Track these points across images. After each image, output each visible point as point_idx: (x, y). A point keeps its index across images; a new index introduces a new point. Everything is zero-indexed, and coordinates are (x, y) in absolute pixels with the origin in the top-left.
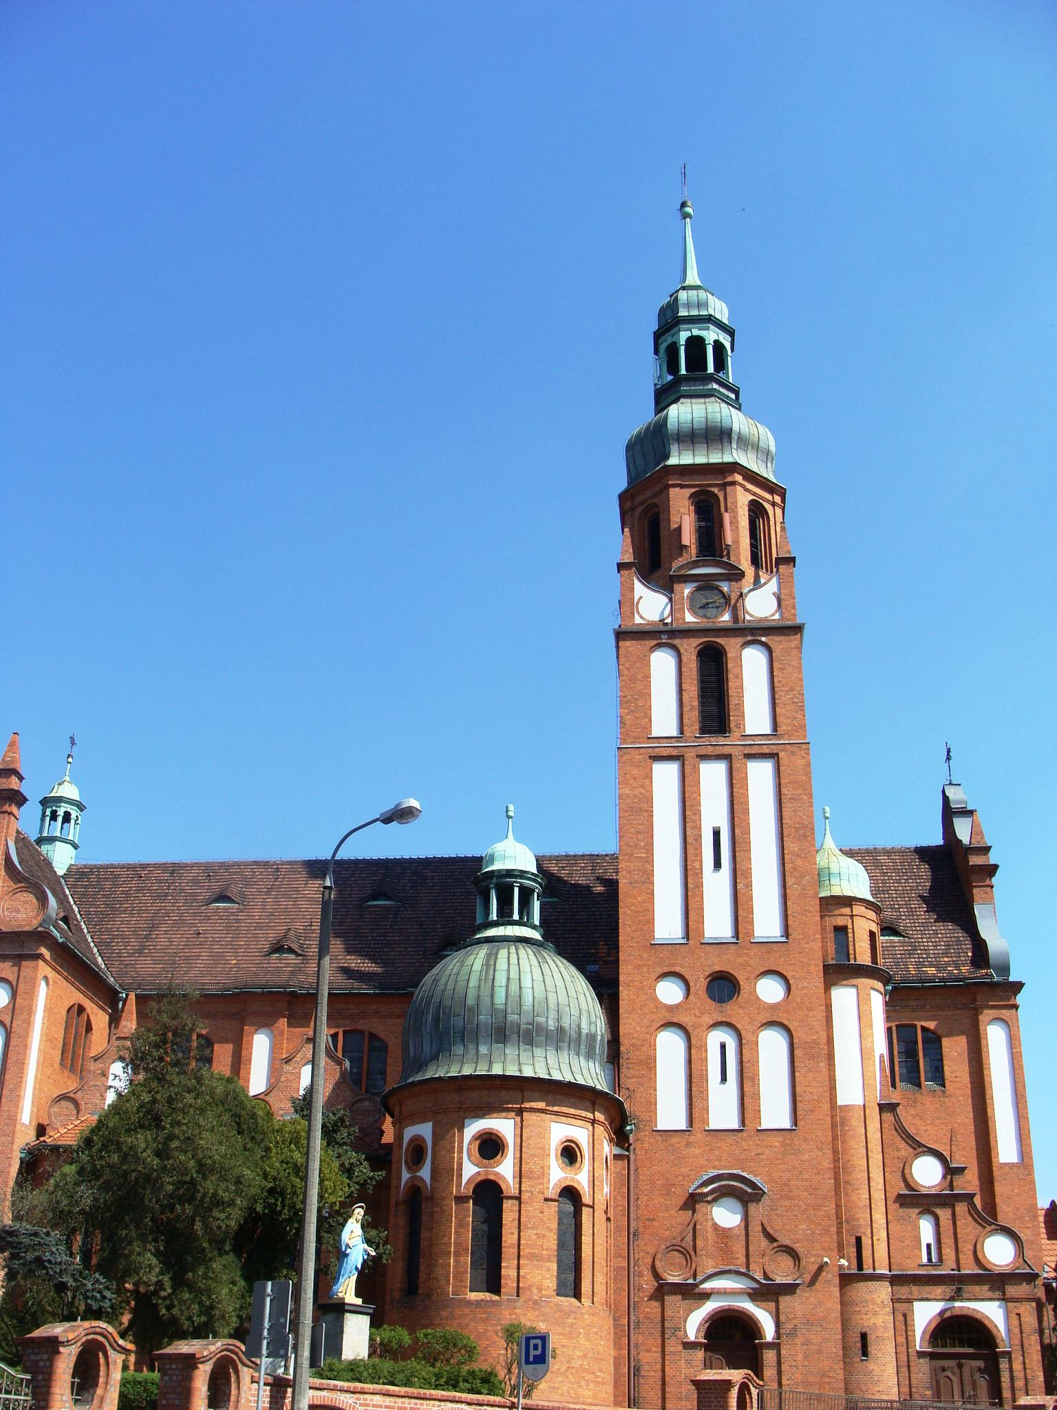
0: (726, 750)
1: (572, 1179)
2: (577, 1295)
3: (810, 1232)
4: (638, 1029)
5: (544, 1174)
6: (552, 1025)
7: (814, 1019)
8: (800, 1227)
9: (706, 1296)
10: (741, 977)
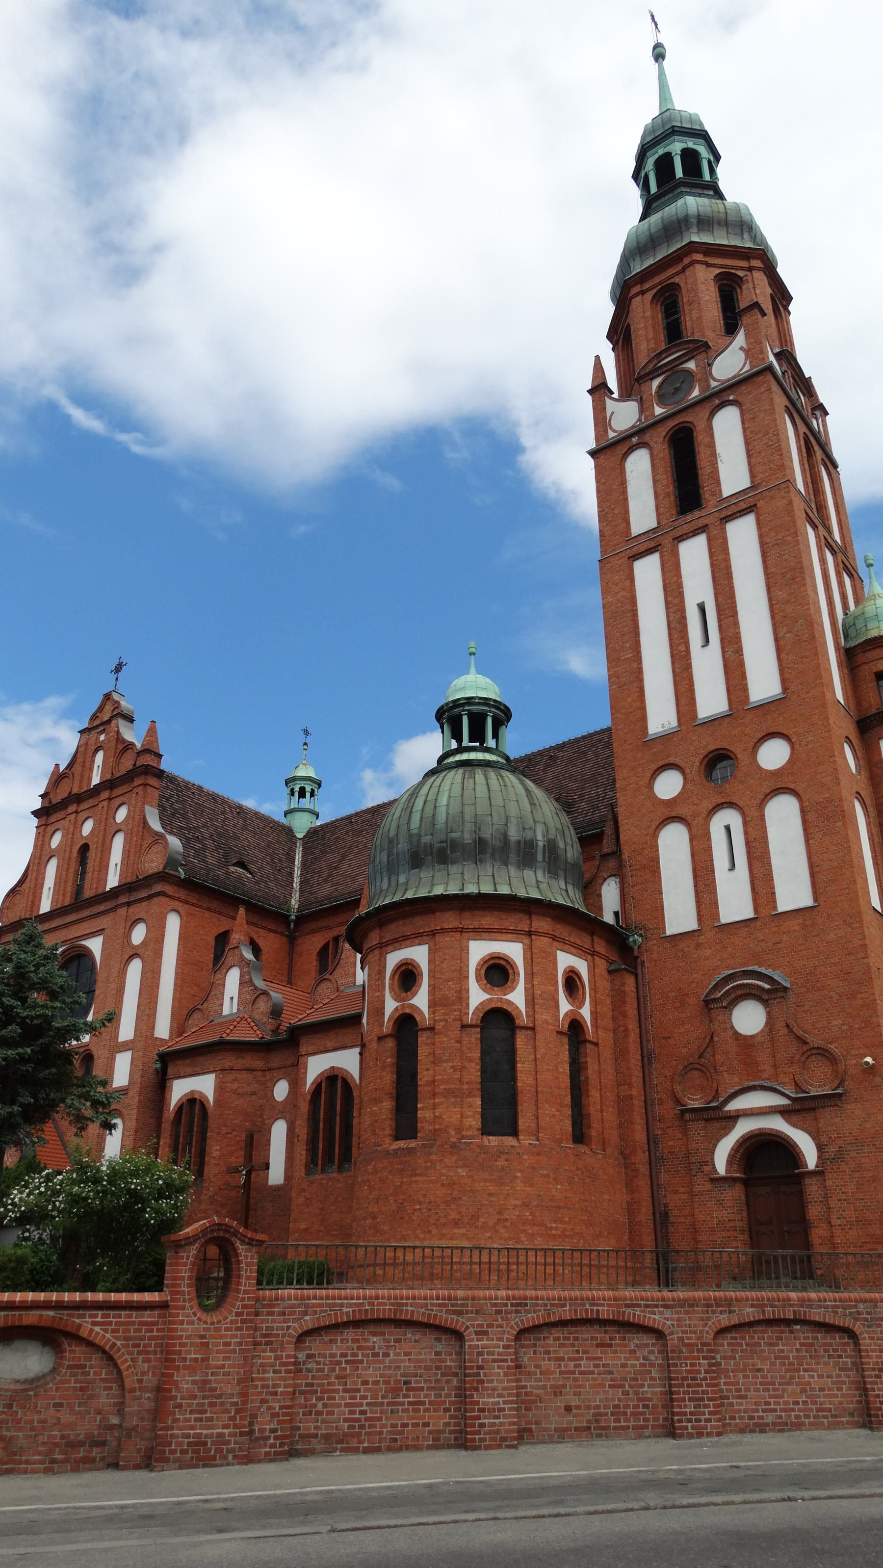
0: (702, 522)
1: (501, 1000)
2: (514, 1132)
3: (845, 1027)
4: (637, 833)
5: (463, 996)
6: (468, 838)
7: (824, 774)
8: (834, 1023)
9: (734, 1117)
10: (737, 749)
